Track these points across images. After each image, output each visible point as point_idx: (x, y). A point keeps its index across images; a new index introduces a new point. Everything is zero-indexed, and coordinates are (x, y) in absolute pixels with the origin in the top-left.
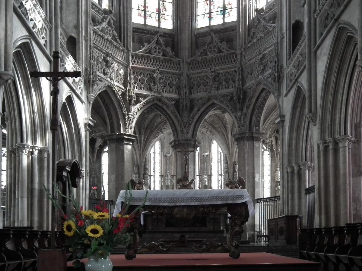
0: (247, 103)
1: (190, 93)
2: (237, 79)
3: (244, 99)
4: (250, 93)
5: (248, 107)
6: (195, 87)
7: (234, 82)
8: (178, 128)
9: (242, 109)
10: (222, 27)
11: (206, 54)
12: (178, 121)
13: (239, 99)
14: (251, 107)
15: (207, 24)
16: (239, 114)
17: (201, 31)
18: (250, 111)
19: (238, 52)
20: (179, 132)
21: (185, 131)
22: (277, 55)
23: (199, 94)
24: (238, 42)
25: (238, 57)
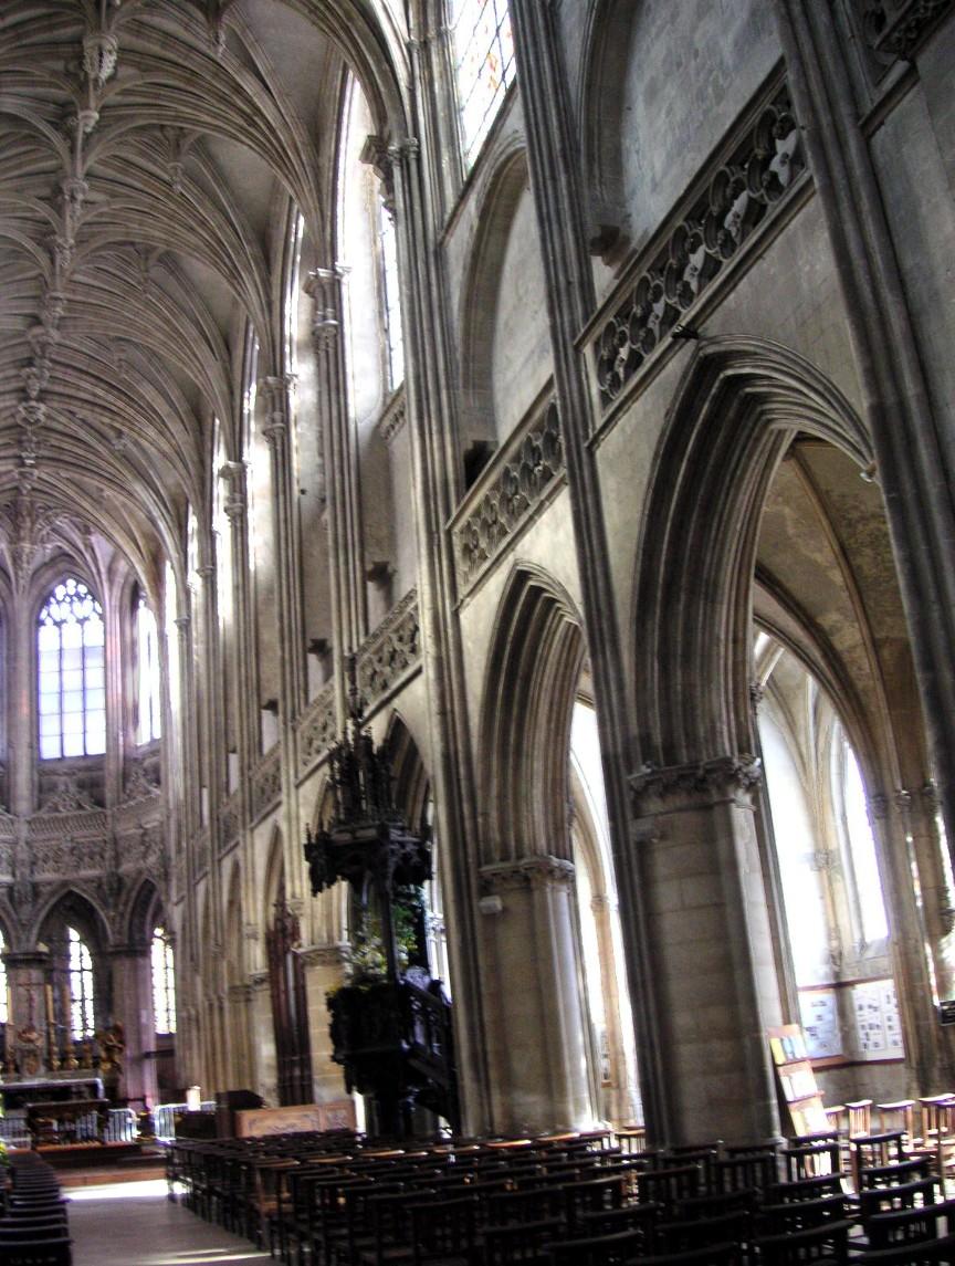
0: (123, 897)
1: (32, 872)
2: (107, 855)
3: (120, 890)
4: (128, 882)
5: (126, 904)
6: (40, 863)
7: (102, 857)
8: (13, 934)
9: (116, 906)
10: (82, 763)
11: (57, 810)
12: (12, 921)
13: (111, 889)
14: (131, 904)
15: (58, 756)
16: (112, 914)
17: (48, 767)
18: (129, 910)
19: (109, 812)
20: (14, 940)
21: (23, 937)
22: (163, 840)
23: (46, 875)
24: (109, 795)
25: (109, 819)
